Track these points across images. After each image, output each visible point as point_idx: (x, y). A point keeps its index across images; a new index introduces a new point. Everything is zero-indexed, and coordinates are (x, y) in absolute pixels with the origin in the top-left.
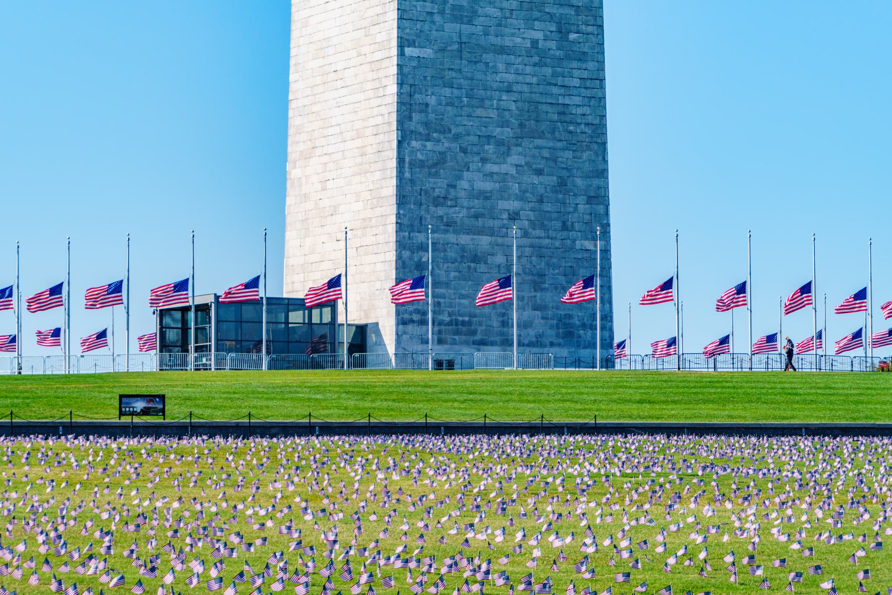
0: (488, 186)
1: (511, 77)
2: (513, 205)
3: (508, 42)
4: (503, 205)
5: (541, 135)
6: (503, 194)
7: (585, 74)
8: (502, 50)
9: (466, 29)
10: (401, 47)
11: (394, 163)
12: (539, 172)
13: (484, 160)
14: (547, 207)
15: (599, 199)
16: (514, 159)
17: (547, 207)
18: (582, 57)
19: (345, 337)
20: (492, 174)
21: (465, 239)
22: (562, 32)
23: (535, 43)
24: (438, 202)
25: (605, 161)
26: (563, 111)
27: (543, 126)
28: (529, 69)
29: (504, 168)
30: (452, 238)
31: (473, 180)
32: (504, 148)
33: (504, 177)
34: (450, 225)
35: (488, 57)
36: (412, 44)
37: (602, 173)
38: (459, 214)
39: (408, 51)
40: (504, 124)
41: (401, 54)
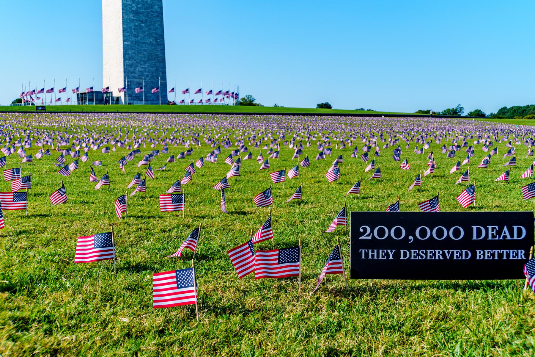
0: (142, 70)
1: (146, 48)
2: (147, 73)
3: (145, 41)
4: (145, 73)
5: (152, 60)
6: (145, 71)
8: (144, 43)
9: (137, 39)
10: (124, 42)
11: (123, 65)
12: (152, 67)
13: (141, 65)
14: (154, 74)
15: (164, 73)
16: (147, 64)
17: (154, 74)
18: (160, 45)
19: (115, 99)
20: (142, 68)
21: (138, 80)
23: (151, 42)
24: (132, 73)
26: (157, 55)
27: (153, 58)
30: (135, 80)
31: (139, 69)
32: (145, 62)
33: (145, 68)
34: (134, 77)
35: (141, 44)
36: (126, 41)
37: (165, 68)
38: (136, 75)
39: (125, 43)
40: (145, 58)
41: (124, 43)
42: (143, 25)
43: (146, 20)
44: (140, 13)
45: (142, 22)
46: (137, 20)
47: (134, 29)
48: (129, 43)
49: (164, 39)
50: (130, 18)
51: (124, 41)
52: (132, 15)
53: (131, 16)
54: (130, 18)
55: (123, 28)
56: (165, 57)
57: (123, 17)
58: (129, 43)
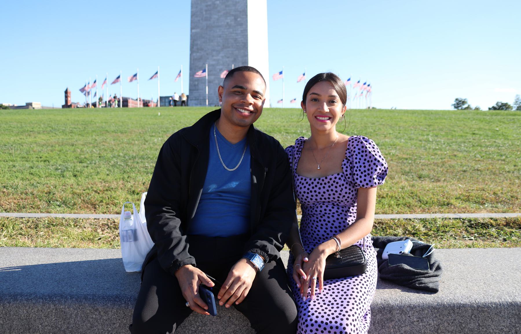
0: (214, 63)
7: (242, 29)
12: (228, 57)
13: (213, 56)
18: (241, 25)
20: (214, 60)
22: (236, 19)
23: (228, 23)
25: (247, 52)
26: (236, 40)
28: (226, 30)
29: (219, 57)
37: (247, 56)
39: (193, 31)
47: (206, 11)
48: (198, 30)
49: (247, 15)
51: (192, 29)
55: (192, 12)
56: (247, 40)
58: (198, 30)
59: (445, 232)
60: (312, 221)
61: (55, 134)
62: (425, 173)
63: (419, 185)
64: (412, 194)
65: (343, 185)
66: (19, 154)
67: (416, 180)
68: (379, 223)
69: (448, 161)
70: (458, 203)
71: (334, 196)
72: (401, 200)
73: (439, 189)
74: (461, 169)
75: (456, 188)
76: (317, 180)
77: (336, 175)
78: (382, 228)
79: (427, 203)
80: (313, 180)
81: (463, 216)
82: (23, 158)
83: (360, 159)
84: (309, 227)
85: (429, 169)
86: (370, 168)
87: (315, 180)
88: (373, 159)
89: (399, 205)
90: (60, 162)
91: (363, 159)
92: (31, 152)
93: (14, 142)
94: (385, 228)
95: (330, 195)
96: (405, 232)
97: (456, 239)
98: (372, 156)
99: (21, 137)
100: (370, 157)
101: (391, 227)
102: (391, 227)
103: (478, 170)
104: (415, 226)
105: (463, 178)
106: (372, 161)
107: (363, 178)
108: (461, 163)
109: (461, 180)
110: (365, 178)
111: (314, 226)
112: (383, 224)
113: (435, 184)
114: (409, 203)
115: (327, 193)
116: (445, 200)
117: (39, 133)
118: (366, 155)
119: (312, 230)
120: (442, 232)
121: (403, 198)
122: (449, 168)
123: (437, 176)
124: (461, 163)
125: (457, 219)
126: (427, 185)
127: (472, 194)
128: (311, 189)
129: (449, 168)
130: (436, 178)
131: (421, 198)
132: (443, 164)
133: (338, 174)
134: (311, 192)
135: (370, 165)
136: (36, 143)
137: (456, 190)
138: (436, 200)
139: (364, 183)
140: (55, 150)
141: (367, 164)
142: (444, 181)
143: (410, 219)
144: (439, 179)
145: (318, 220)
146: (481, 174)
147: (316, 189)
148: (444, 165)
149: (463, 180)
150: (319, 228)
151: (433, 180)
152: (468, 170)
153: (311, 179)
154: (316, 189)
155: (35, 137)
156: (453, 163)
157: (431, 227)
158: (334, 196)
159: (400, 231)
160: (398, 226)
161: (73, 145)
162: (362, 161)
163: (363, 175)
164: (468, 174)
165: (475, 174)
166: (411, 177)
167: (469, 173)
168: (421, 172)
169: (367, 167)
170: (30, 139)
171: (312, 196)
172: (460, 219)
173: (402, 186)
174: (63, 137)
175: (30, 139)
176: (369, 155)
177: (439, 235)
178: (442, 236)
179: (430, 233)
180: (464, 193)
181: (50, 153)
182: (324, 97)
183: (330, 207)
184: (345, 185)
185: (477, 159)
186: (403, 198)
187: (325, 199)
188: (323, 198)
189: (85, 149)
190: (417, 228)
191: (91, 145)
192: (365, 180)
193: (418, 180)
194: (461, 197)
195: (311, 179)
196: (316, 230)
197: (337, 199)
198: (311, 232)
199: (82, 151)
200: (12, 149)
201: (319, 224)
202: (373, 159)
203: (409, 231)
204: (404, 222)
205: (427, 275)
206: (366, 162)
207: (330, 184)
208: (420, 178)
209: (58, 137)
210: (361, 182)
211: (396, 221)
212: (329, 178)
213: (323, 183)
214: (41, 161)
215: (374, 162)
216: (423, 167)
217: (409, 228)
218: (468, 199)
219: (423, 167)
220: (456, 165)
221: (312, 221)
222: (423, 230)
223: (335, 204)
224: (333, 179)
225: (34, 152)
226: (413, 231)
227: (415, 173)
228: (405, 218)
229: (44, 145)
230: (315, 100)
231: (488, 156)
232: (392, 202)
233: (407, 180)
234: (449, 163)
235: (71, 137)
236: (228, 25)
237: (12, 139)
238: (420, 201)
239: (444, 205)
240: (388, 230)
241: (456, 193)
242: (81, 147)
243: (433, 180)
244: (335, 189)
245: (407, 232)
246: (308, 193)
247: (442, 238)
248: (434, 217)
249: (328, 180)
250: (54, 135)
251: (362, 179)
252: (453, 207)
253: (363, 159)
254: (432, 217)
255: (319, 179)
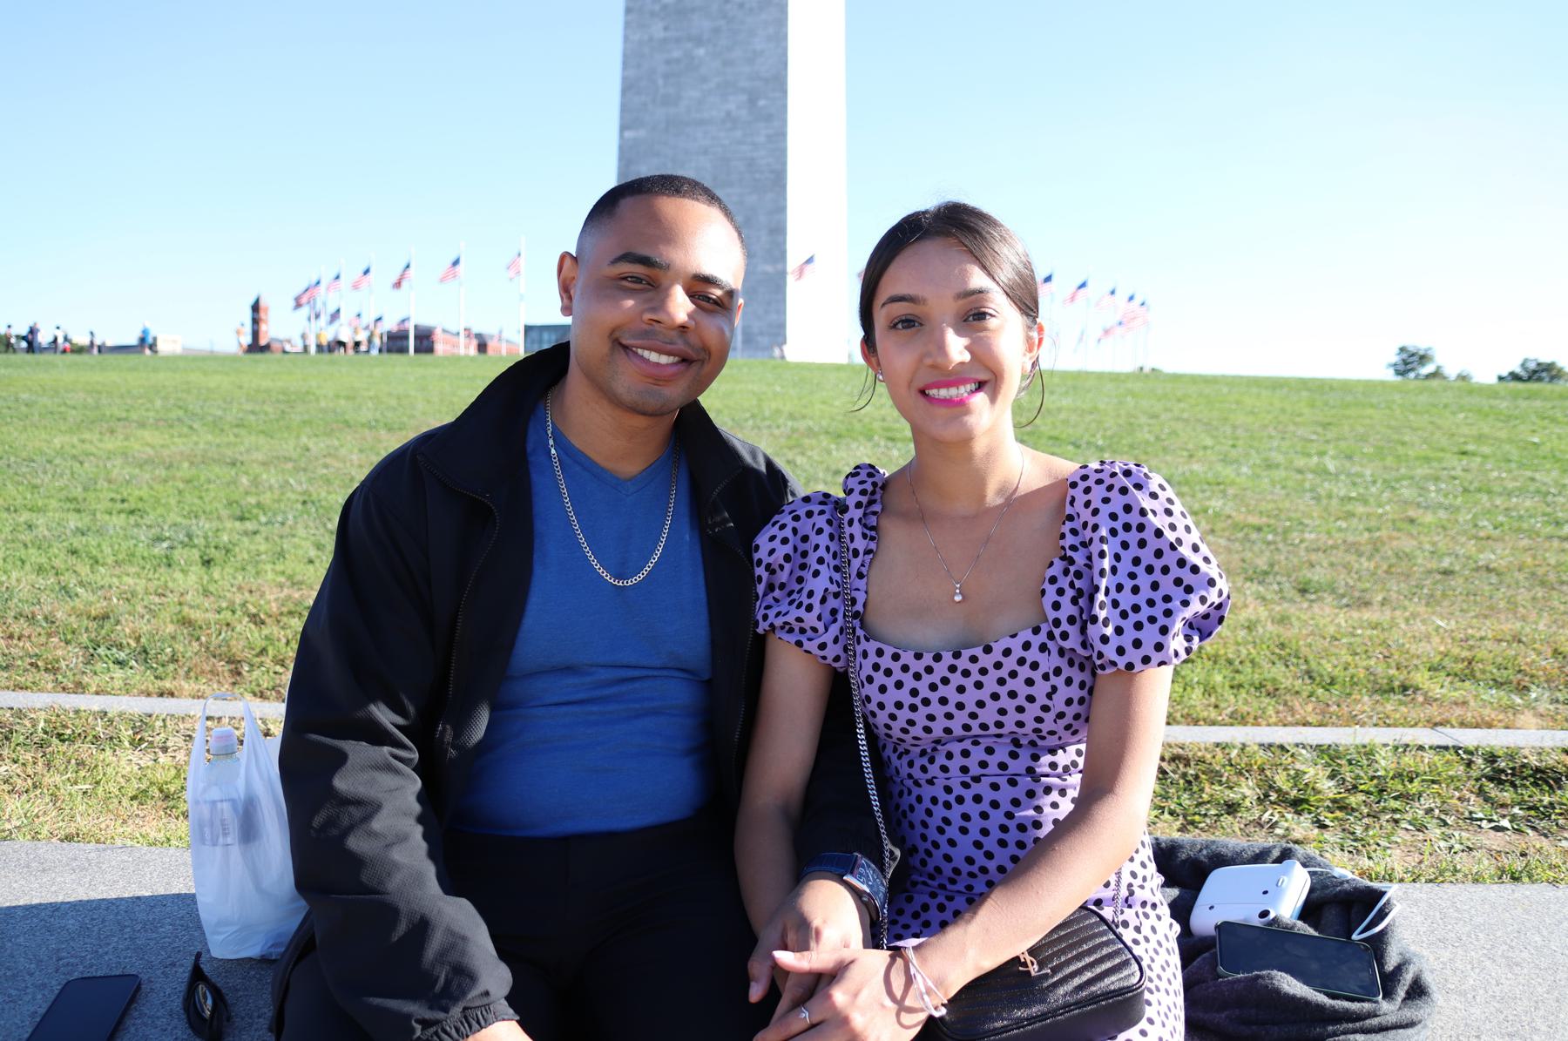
18: (769, 118)
22: (752, 102)
23: (728, 113)
37: (782, 209)
39: (627, 134)
42: (701, 52)
43: (716, 31)
44: (693, 10)
45: (699, 41)
46: (678, 40)
47: (666, 76)
48: (642, 133)
49: (785, 92)
50: (651, 39)
52: (661, 25)
53: (657, 30)
54: (651, 39)
55: (624, 79)
56: (784, 164)
57: (626, 39)
58: (642, 133)
59: (1404, 797)
60: (927, 803)
61: (191, 428)
62: (1318, 575)
63: (1304, 617)
64: (1284, 653)
65: (1058, 672)
66: (62, 489)
67: (1292, 601)
68: (1175, 759)
69: (1391, 538)
70: (1437, 687)
71: (1020, 717)
72: (1248, 668)
73: (1369, 632)
74: (1433, 565)
75: (1428, 631)
76: (948, 659)
77: (1026, 635)
78: (1184, 775)
79: (1332, 683)
80: (928, 659)
81: (1469, 738)
82: (69, 500)
83: (1117, 557)
84: (912, 826)
85: (1332, 565)
86: (1157, 596)
87: (937, 658)
88: (1169, 559)
89: (1240, 686)
90: (174, 517)
91: (1127, 557)
92: (102, 484)
93: (60, 453)
94: (1197, 777)
95: (1002, 712)
96: (1267, 796)
97: (1445, 824)
98: (1166, 549)
99: (87, 436)
100: (1159, 554)
101: (1215, 777)
102: (1215, 777)
103: (1488, 569)
104: (1299, 774)
105: (1444, 596)
106: (1165, 570)
107: (1130, 634)
108: (1434, 544)
109: (1439, 603)
110: (1139, 635)
111: (935, 821)
112: (1187, 765)
113: (1355, 615)
114: (1274, 680)
115: (992, 706)
116: (1393, 672)
117: (142, 425)
118: (1142, 544)
119: (924, 837)
120: (1395, 798)
121: (1252, 661)
122: (1394, 561)
123: (1360, 585)
124: (1434, 544)
125: (1446, 748)
126: (1328, 616)
127: (1481, 654)
128: (924, 692)
129: (1394, 561)
130: (1357, 594)
131: (1313, 665)
132: (1376, 546)
133: (1036, 631)
134: (926, 702)
135: (1155, 586)
136: (125, 455)
137: (1428, 637)
138: (1362, 674)
139: (1134, 655)
140: (174, 478)
141: (1144, 581)
142: (1384, 603)
143: (1282, 747)
144: (1367, 596)
145: (951, 798)
146: (1501, 582)
147: (949, 691)
148: (1377, 550)
149: (1445, 603)
150: (952, 832)
151: (1345, 601)
152: (1457, 568)
153: (918, 656)
154: (949, 691)
155: (127, 438)
156: (1407, 544)
157: (1358, 777)
158: (1020, 717)
159: (1248, 792)
160: (1241, 774)
161: (234, 464)
162: (1125, 566)
163: (1127, 625)
164: (1457, 582)
165: (1483, 584)
166: (1276, 587)
167: (1461, 580)
168: (1307, 574)
169: (1146, 592)
170: (110, 444)
171: (931, 718)
172: (1456, 749)
173: (1249, 620)
174: (210, 437)
175: (110, 444)
176: (1153, 544)
177: (1384, 810)
178: (1395, 811)
179: (1353, 800)
180: (1456, 651)
181: (156, 486)
182: (941, 304)
183: (1001, 755)
184: (1067, 672)
185: (1482, 534)
186: (1252, 661)
187: (984, 727)
188: (974, 724)
189: (265, 476)
190: (1306, 778)
191: (290, 466)
192: (1137, 644)
193: (1298, 598)
194: (1446, 662)
195: (918, 656)
196: (942, 840)
197: (1031, 725)
198: (922, 846)
199: (255, 482)
200: (45, 472)
201: (955, 814)
202: (1169, 559)
203: (1279, 791)
204: (1261, 757)
205: (1375, 1021)
206: (1140, 570)
207: (1004, 673)
208: (1303, 591)
209: (195, 438)
210: (1121, 651)
211: (1234, 753)
212: (998, 649)
213: (974, 668)
214: (120, 512)
215: (1175, 572)
216: (1313, 557)
217: (1281, 780)
218: (1467, 673)
219: (1313, 557)
220: (1418, 552)
221: (927, 803)
222: (1328, 788)
223: (1024, 741)
224: (1018, 652)
225: (110, 482)
226: (1294, 793)
227: (1289, 576)
228: (1266, 741)
229: (146, 462)
230: (909, 322)
231: (1516, 525)
232: (1218, 678)
233: (1264, 599)
234: (1395, 543)
235: (232, 438)
236: (730, 119)
237: (57, 442)
238: (1309, 673)
239: (1392, 690)
240: (1207, 789)
241: (1432, 649)
242: (257, 469)
243: (1345, 601)
244: (1024, 691)
245: (1273, 797)
246: (913, 708)
247: (1396, 821)
248: (1366, 741)
249: (996, 655)
250: (185, 430)
251: (1126, 640)
252: (1421, 699)
253: (1127, 557)
254: (1358, 742)
255: (957, 655)
